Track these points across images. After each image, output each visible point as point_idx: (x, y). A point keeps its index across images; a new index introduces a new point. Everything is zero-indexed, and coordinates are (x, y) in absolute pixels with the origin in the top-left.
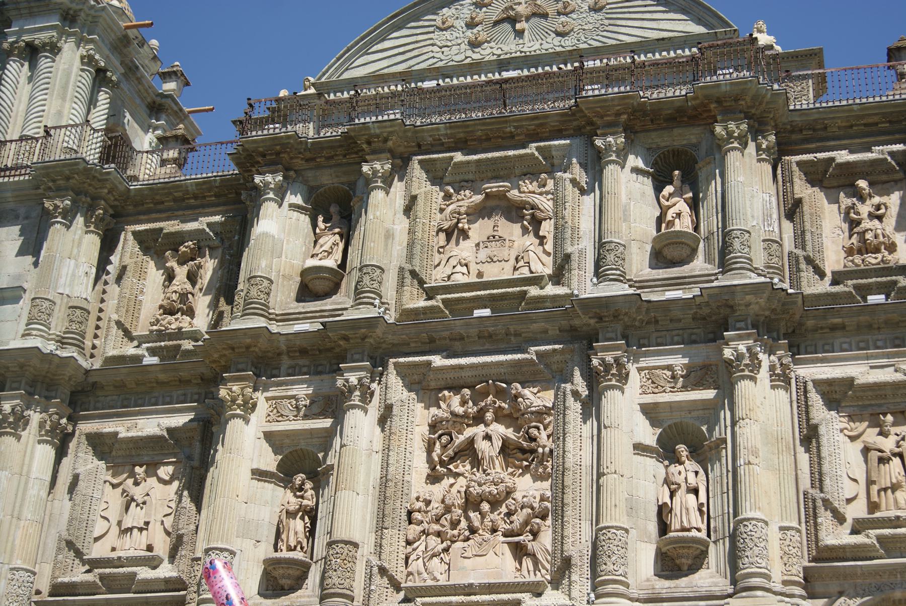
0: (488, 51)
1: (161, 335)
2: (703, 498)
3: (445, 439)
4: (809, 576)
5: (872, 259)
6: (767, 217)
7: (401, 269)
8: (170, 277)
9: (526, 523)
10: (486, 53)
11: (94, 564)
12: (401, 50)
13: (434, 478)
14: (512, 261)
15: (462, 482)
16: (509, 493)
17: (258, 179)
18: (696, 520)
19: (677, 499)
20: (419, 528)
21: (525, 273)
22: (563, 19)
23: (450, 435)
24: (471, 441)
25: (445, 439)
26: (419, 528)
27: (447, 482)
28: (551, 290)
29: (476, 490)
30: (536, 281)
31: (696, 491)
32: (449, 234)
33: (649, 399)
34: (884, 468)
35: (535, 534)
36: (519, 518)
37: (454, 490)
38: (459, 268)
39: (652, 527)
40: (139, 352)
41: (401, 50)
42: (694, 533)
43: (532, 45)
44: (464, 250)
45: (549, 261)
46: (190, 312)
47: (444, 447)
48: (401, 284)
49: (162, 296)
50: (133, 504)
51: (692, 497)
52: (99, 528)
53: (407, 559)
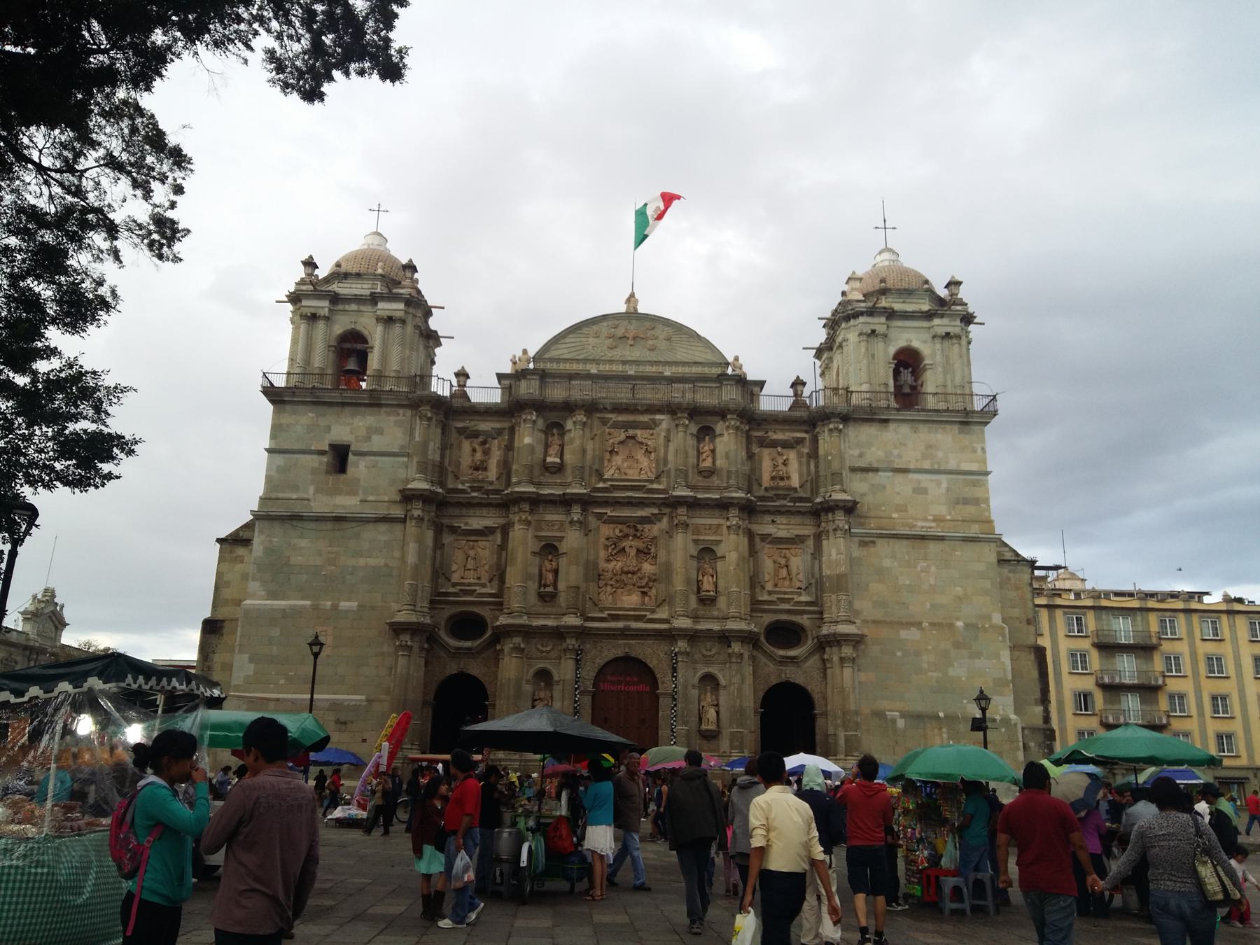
0: (615, 353)
1: (474, 481)
2: (715, 580)
3: (613, 546)
4: (752, 610)
5: (782, 484)
6: (743, 464)
7: (590, 468)
8: (474, 450)
9: (647, 583)
10: (617, 354)
11: (454, 585)
12: (574, 345)
13: (608, 561)
14: (638, 470)
15: (620, 564)
16: (639, 570)
17: (524, 417)
18: (711, 587)
19: (706, 577)
20: (604, 582)
21: (643, 477)
22: (651, 342)
23: (615, 544)
24: (624, 548)
25: (613, 546)
26: (604, 582)
27: (614, 563)
28: (655, 486)
29: (625, 569)
30: (651, 482)
31: (713, 576)
32: (611, 452)
33: (696, 537)
34: (781, 570)
35: (651, 588)
36: (644, 582)
37: (618, 566)
38: (617, 471)
39: (695, 589)
40: (464, 487)
41: (574, 345)
42: (712, 593)
43: (636, 353)
44: (618, 460)
45: (654, 470)
46: (485, 469)
47: (613, 549)
48: (590, 476)
49: (470, 459)
50: (469, 559)
51: (710, 579)
52: (454, 567)
53: (599, 594)
